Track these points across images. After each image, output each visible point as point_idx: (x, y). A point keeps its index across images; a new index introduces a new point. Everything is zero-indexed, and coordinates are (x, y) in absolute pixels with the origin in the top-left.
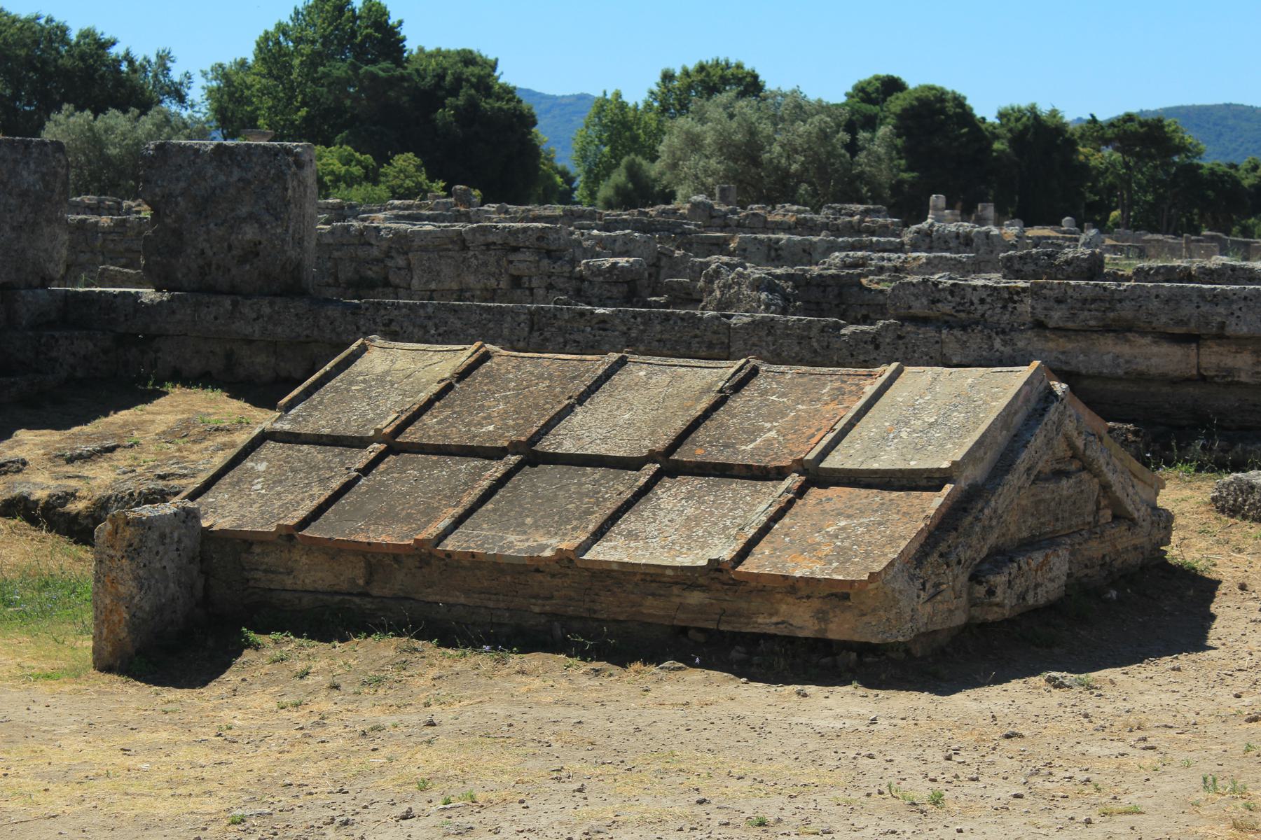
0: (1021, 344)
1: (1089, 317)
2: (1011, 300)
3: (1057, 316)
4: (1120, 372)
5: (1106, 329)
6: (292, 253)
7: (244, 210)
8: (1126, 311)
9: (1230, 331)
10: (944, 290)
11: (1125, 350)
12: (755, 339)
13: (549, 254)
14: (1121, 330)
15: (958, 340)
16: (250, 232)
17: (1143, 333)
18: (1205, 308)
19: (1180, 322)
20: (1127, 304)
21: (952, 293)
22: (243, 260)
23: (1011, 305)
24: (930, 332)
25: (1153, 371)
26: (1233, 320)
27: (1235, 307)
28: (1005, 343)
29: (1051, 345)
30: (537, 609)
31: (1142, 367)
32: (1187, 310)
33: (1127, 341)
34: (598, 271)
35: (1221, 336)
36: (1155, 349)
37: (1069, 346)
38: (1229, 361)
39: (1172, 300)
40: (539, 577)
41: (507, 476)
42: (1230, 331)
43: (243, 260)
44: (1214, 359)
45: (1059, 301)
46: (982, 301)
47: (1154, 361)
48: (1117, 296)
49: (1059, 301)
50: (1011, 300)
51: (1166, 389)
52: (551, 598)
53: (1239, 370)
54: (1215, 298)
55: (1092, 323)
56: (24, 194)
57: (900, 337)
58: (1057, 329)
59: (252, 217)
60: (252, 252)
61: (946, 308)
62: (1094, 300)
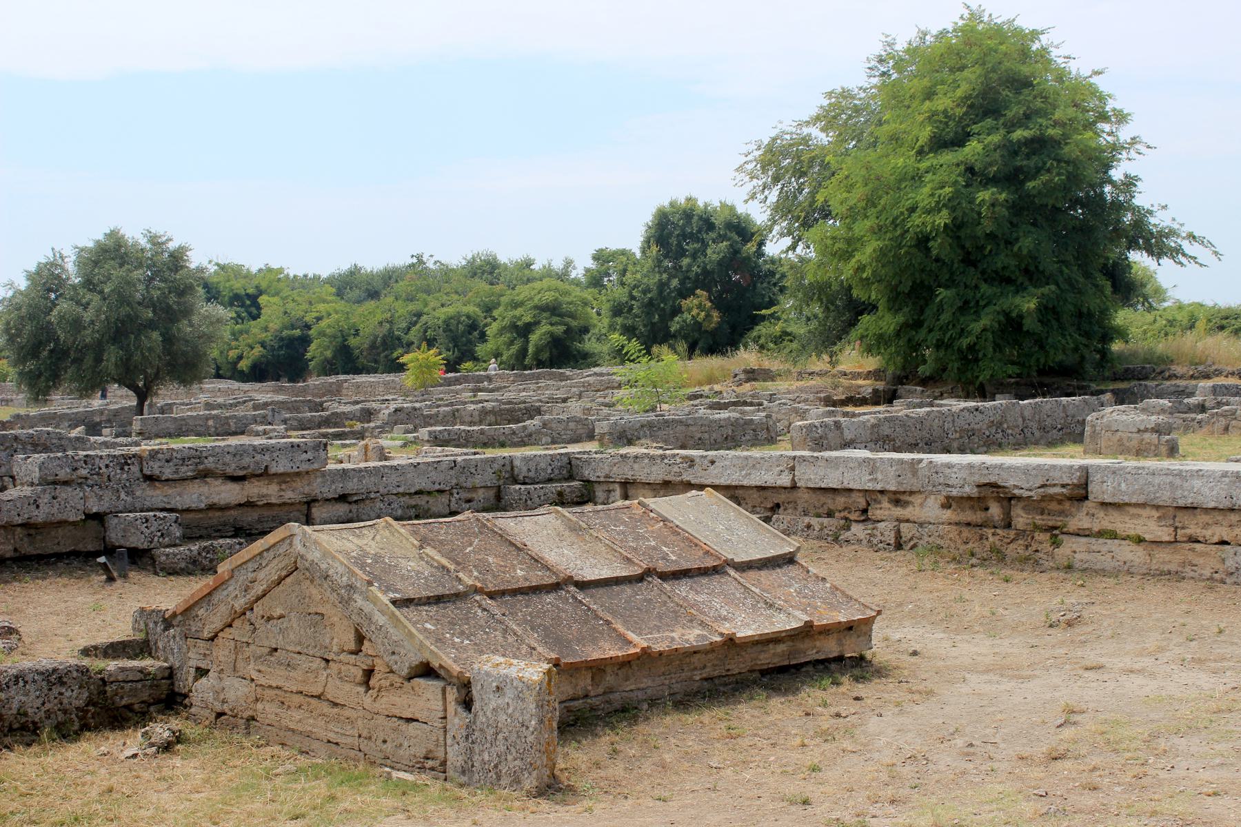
0: (138, 493)
1: (187, 471)
3: (168, 473)
4: (203, 506)
8: (209, 463)
9: (273, 470)
11: (205, 489)
14: (204, 475)
15: (96, 495)
18: (258, 457)
20: (211, 459)
21: (85, 462)
23: (126, 468)
25: (222, 502)
26: (274, 463)
27: (275, 455)
28: (127, 494)
29: (158, 492)
30: (698, 678)
31: (216, 501)
32: (247, 460)
33: (207, 483)
36: (223, 488)
37: (170, 492)
38: (264, 491)
40: (698, 656)
42: (273, 470)
44: (256, 491)
46: (107, 466)
47: (223, 496)
48: (204, 454)
49: (168, 461)
51: (218, 514)
52: (705, 667)
53: (270, 496)
55: (189, 474)
57: (54, 498)
58: (167, 480)
62: (189, 459)
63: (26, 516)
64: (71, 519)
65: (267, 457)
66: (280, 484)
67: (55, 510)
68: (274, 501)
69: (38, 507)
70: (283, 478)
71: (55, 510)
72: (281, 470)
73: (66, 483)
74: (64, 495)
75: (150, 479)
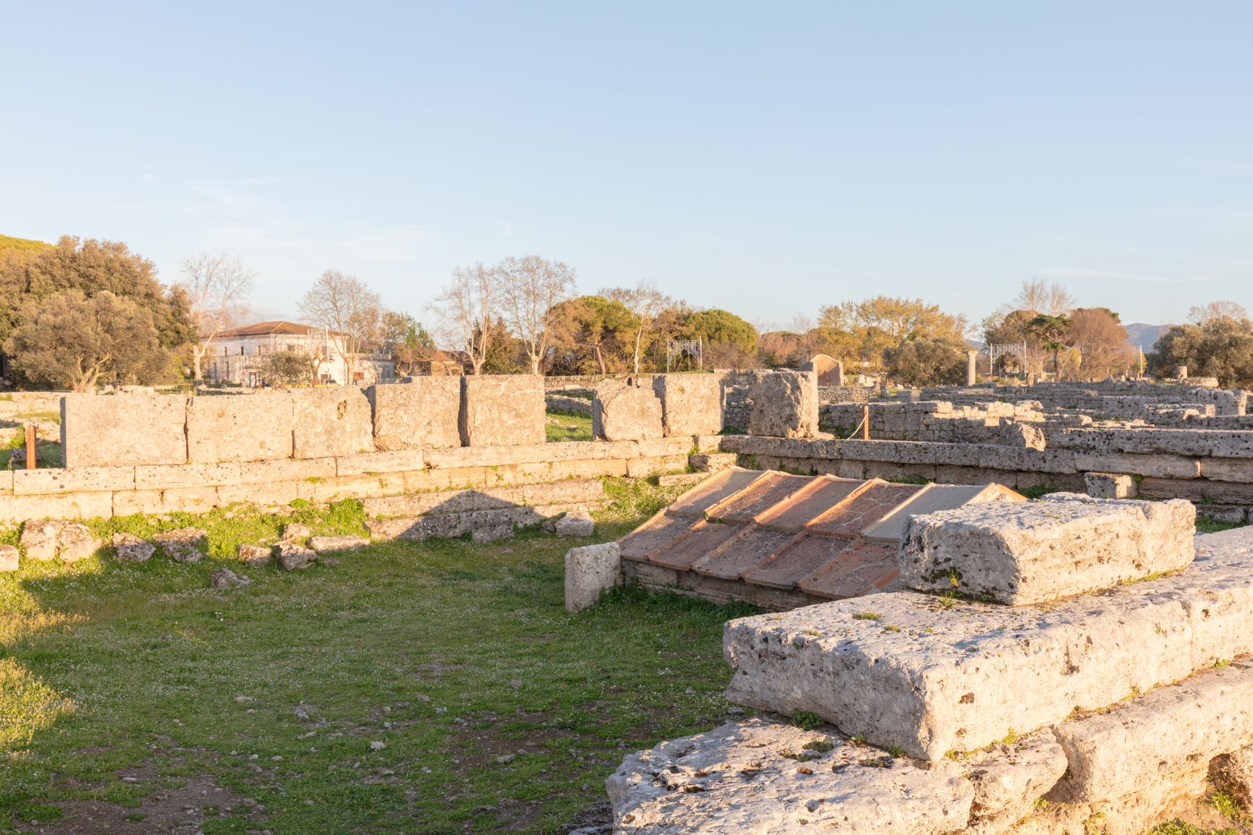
5: (1151, 454)
8: (1162, 445)
9: (1214, 454)
11: (1163, 463)
14: (1160, 452)
17: (1172, 454)
18: (1202, 443)
19: (1190, 450)
24: (1067, 454)
32: (1192, 445)
35: (1210, 456)
36: (1178, 463)
38: (1217, 470)
39: (1184, 438)
42: (1214, 454)
45: (1129, 439)
49: (1129, 439)
54: (1206, 437)
65: (1210, 443)
66: (1231, 466)
68: (1224, 478)
70: (1233, 460)
72: (1221, 454)
73: (1068, 448)
75: (1121, 451)
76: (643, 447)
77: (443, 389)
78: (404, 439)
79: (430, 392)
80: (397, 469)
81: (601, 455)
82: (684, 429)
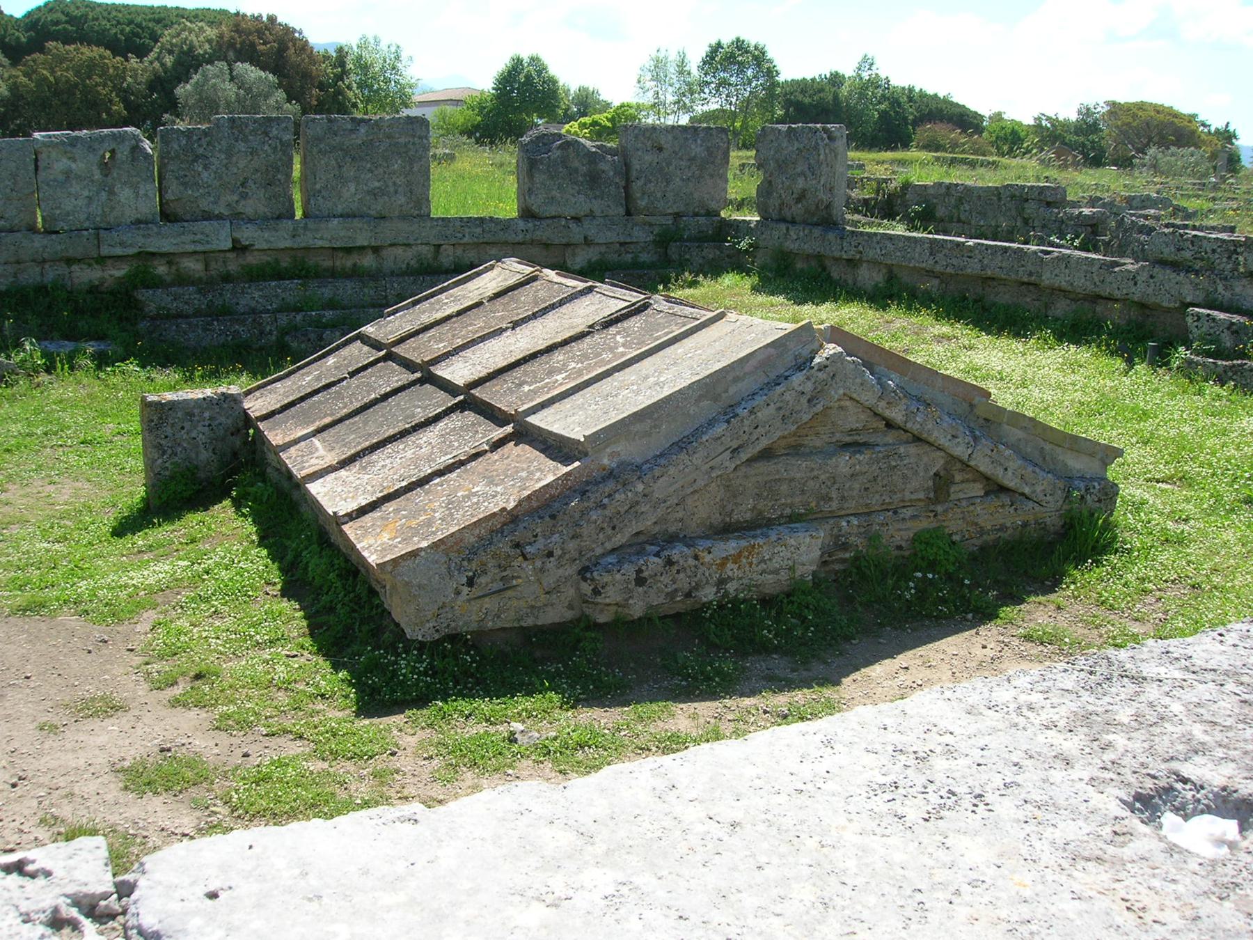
0: (1238, 290)
2: (1235, 252)
6: (822, 196)
7: (799, 170)
10: (1187, 240)
12: (1057, 271)
13: (1049, 204)
16: (801, 183)
21: (1192, 243)
22: (798, 200)
28: (1226, 288)
34: (1071, 218)
41: (413, 383)
43: (798, 200)
46: (1214, 251)
50: (1235, 252)
56: (692, 159)
57: (1152, 277)
59: (803, 174)
60: (801, 197)
61: (1187, 255)
63: (1125, 291)
64: (1165, 304)
67: (1150, 291)
69: (1136, 284)
71: (1150, 291)
74: (1161, 276)
76: (591, 229)
77: (266, 134)
78: (205, 204)
79: (245, 140)
80: (191, 248)
81: (520, 238)
82: (661, 205)
